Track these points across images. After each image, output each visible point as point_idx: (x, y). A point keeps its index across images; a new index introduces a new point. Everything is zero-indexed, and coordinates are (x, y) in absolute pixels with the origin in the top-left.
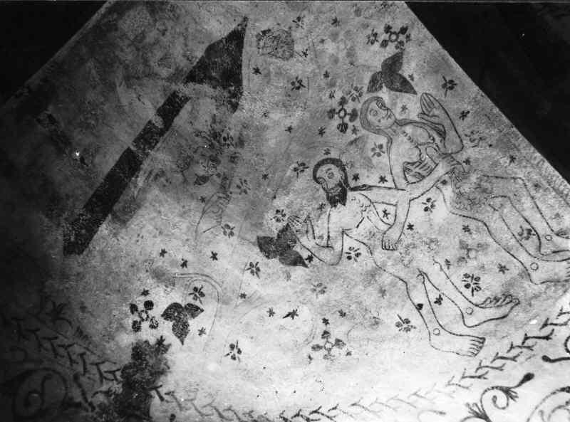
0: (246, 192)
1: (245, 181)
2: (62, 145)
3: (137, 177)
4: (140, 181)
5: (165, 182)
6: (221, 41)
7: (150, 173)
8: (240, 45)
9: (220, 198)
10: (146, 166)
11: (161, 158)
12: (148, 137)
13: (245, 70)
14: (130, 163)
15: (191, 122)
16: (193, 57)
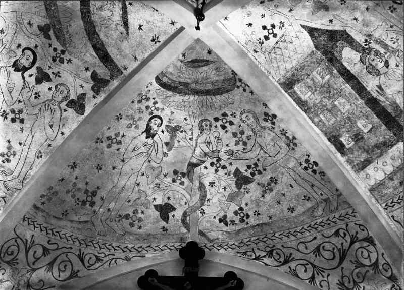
0: (398, 40)
1: (392, 38)
2: (359, 137)
3: (379, 100)
4: (381, 98)
5: (384, 86)
6: (313, 41)
7: (378, 92)
8: (316, 30)
9: (398, 56)
10: (375, 95)
11: (371, 84)
12: (360, 89)
13: (330, 28)
14: (373, 103)
15: (355, 64)
16: (321, 59)
